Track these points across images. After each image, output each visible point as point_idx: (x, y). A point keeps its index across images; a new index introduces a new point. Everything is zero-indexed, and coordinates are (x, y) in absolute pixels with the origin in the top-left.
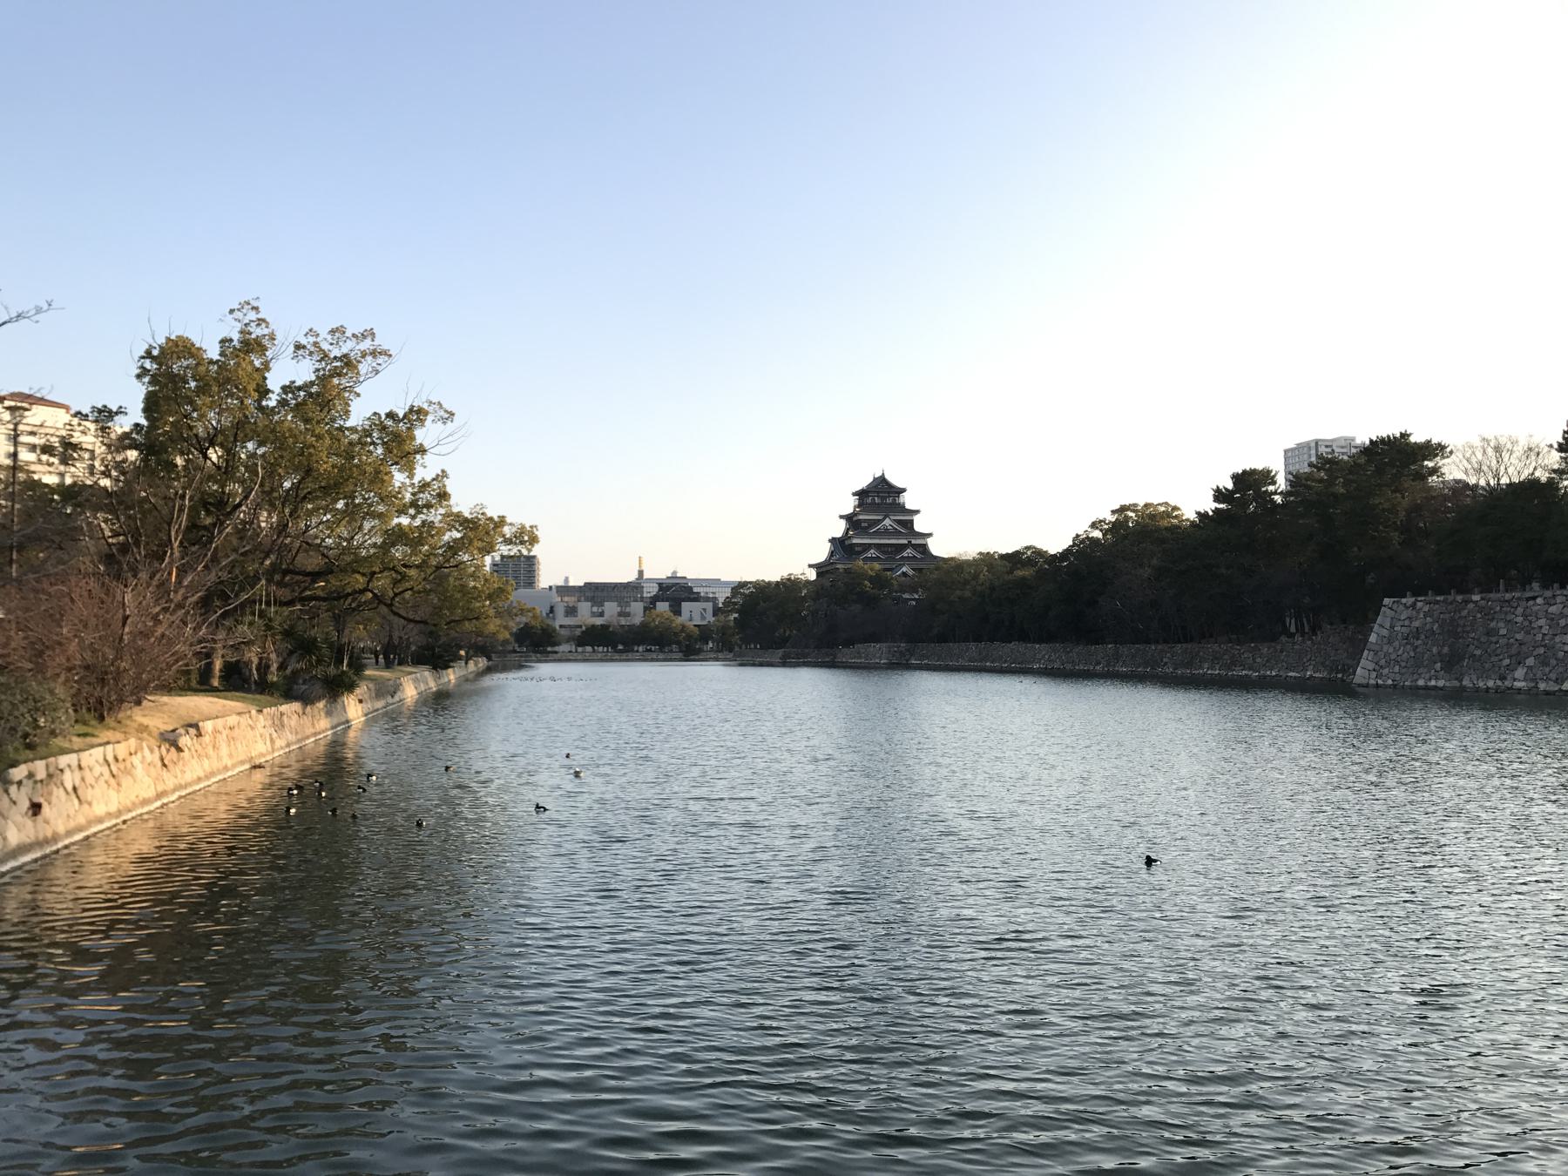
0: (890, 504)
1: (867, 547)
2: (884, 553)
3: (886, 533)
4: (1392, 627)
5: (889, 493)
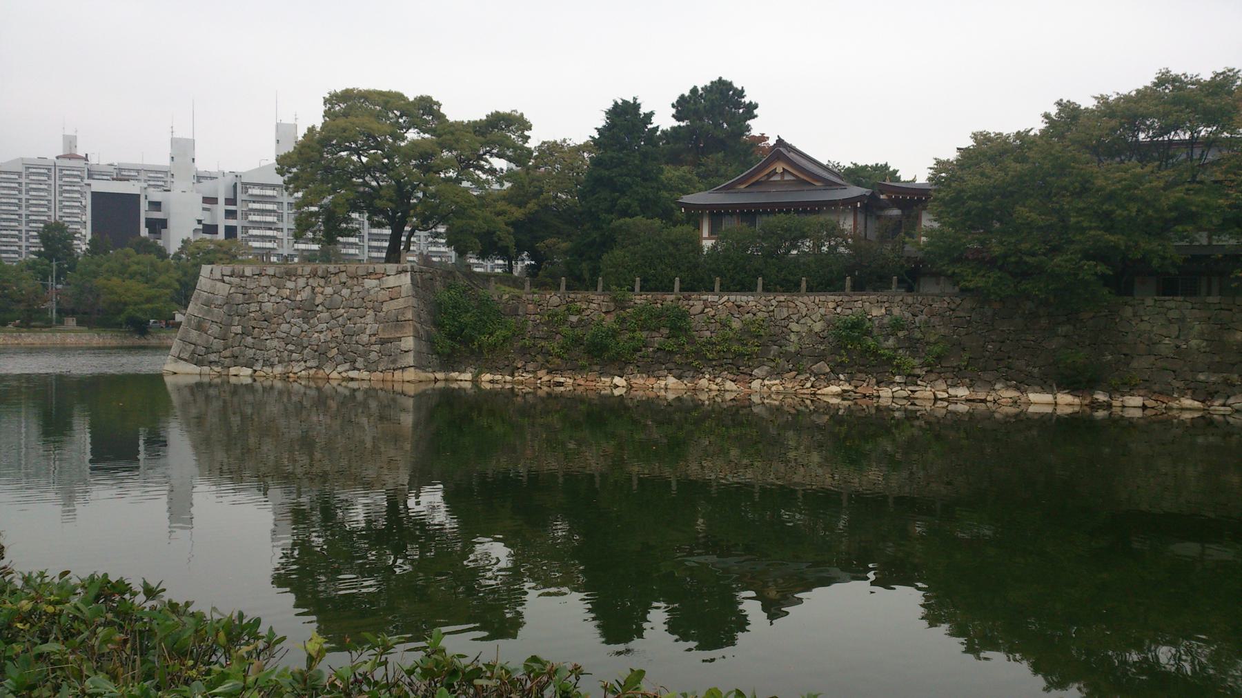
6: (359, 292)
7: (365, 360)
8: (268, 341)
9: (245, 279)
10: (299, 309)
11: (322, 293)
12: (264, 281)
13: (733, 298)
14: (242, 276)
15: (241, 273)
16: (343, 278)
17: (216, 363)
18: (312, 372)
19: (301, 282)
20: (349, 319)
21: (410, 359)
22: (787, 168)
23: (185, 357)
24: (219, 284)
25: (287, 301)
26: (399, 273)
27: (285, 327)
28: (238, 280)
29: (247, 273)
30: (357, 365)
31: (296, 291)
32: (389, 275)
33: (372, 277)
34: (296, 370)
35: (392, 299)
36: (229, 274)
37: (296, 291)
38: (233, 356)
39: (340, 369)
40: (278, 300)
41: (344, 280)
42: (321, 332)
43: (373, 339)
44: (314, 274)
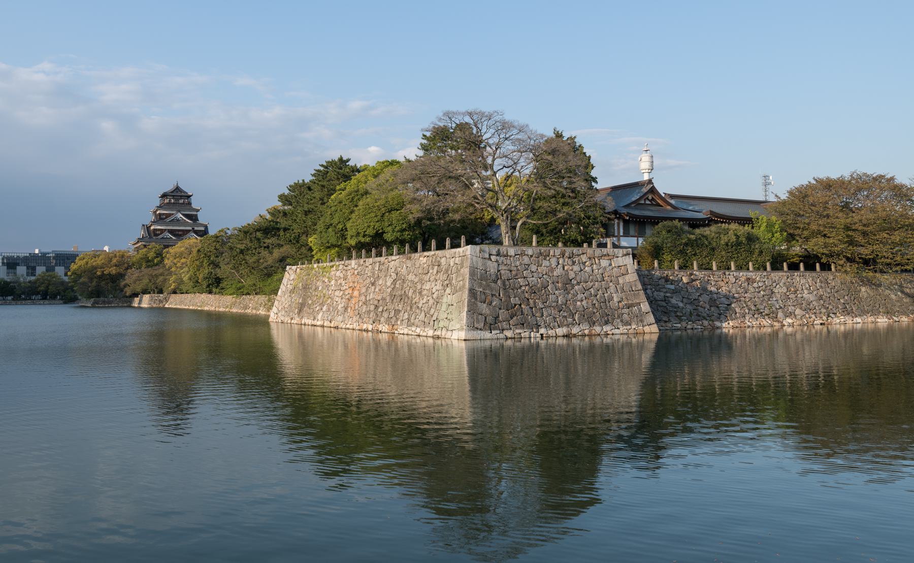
0: (181, 204)
1: (162, 231)
2: (174, 235)
3: (177, 221)
4: (287, 285)
5: (181, 196)
11: (572, 270)
15: (505, 253)
19: (553, 261)
21: (651, 318)
23: (479, 327)
42: (582, 301)
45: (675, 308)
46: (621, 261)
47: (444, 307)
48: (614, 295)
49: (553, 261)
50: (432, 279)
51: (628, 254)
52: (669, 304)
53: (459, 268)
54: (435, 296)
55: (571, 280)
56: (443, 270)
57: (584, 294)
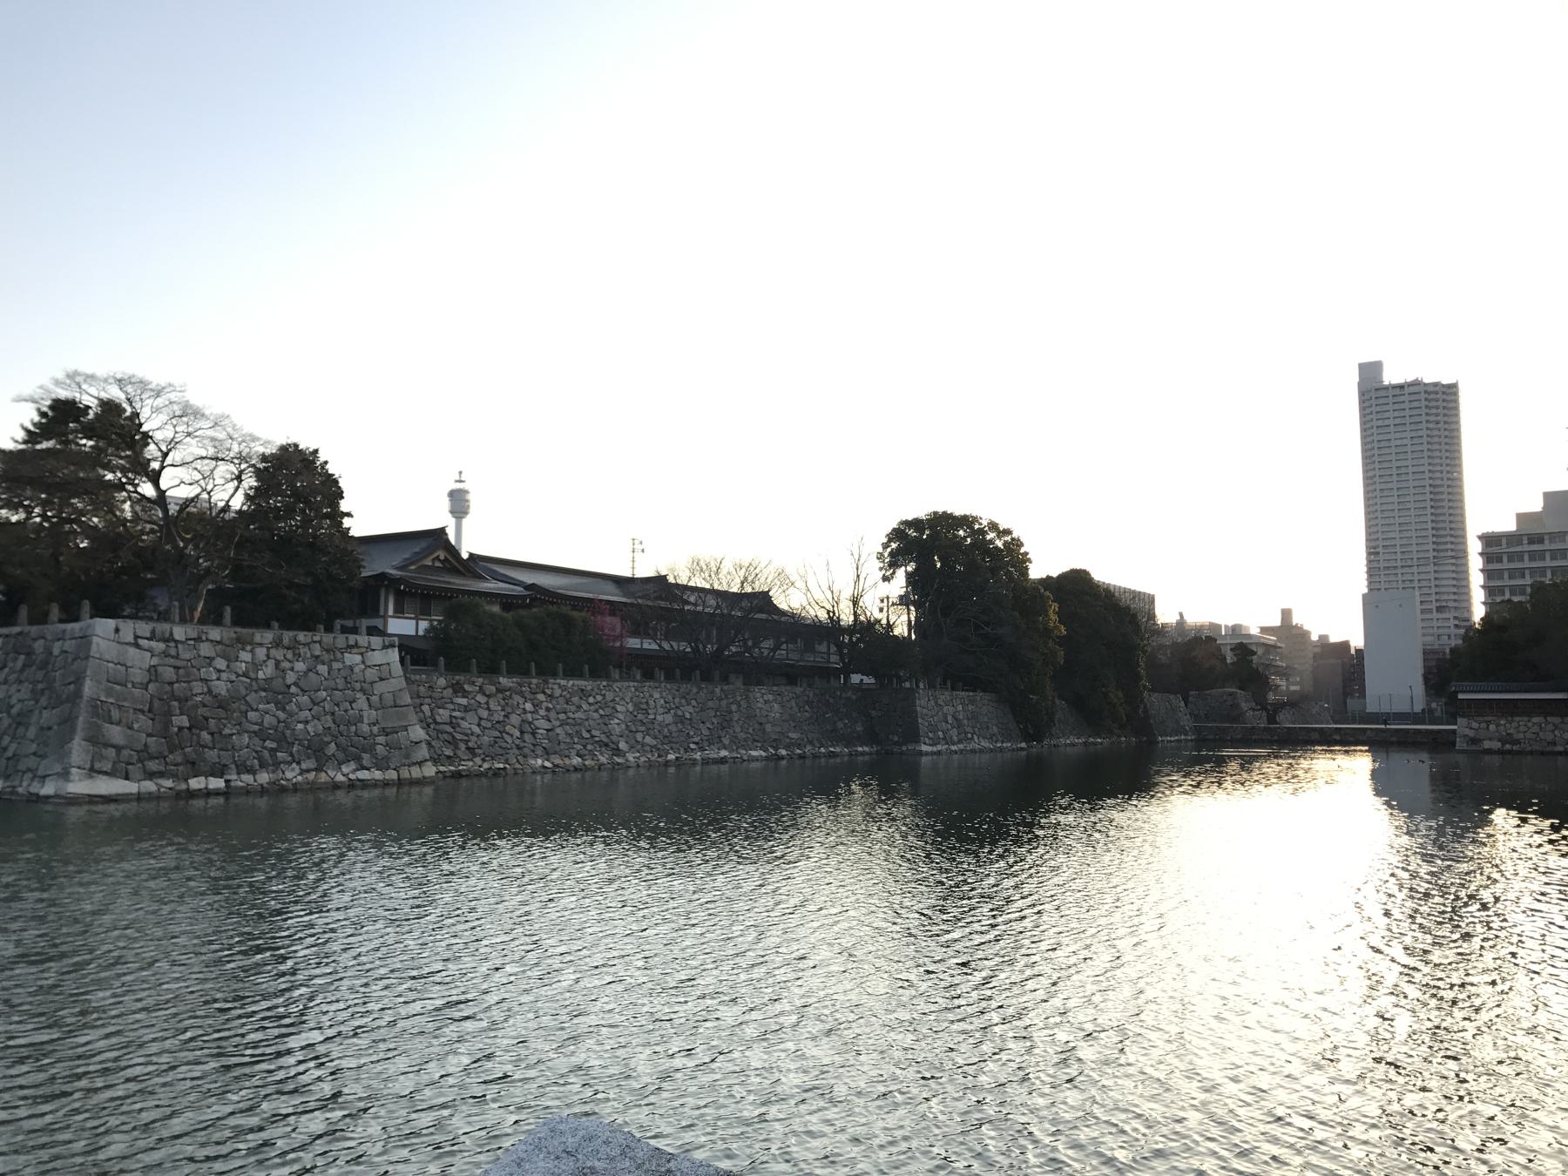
6: (339, 670)
7: (374, 756)
8: (234, 737)
9: (172, 644)
10: (265, 690)
12: (206, 650)
13: (576, 682)
14: (169, 639)
15: (167, 635)
16: (317, 650)
17: (161, 775)
18: (311, 776)
19: (261, 653)
20: (338, 705)
21: (423, 752)
22: (448, 557)
23: (105, 769)
24: (132, 651)
25: (244, 679)
26: (385, 647)
27: (251, 715)
28: (162, 646)
29: (177, 637)
30: (365, 763)
31: (256, 666)
32: (374, 650)
33: (355, 650)
34: (289, 775)
35: (382, 679)
36: (148, 635)
37: (256, 666)
38: (188, 762)
39: (345, 769)
40: (233, 677)
41: (317, 653)
42: (307, 722)
43: (375, 729)
44: (277, 644)
45: (467, 735)
46: (377, 657)
47: (32, 732)
48: (365, 714)
49: (261, 653)
50: (13, 677)
51: (392, 646)
52: (458, 729)
53: (70, 660)
54: (14, 711)
55: (289, 687)
56: (37, 662)
57: (310, 710)
